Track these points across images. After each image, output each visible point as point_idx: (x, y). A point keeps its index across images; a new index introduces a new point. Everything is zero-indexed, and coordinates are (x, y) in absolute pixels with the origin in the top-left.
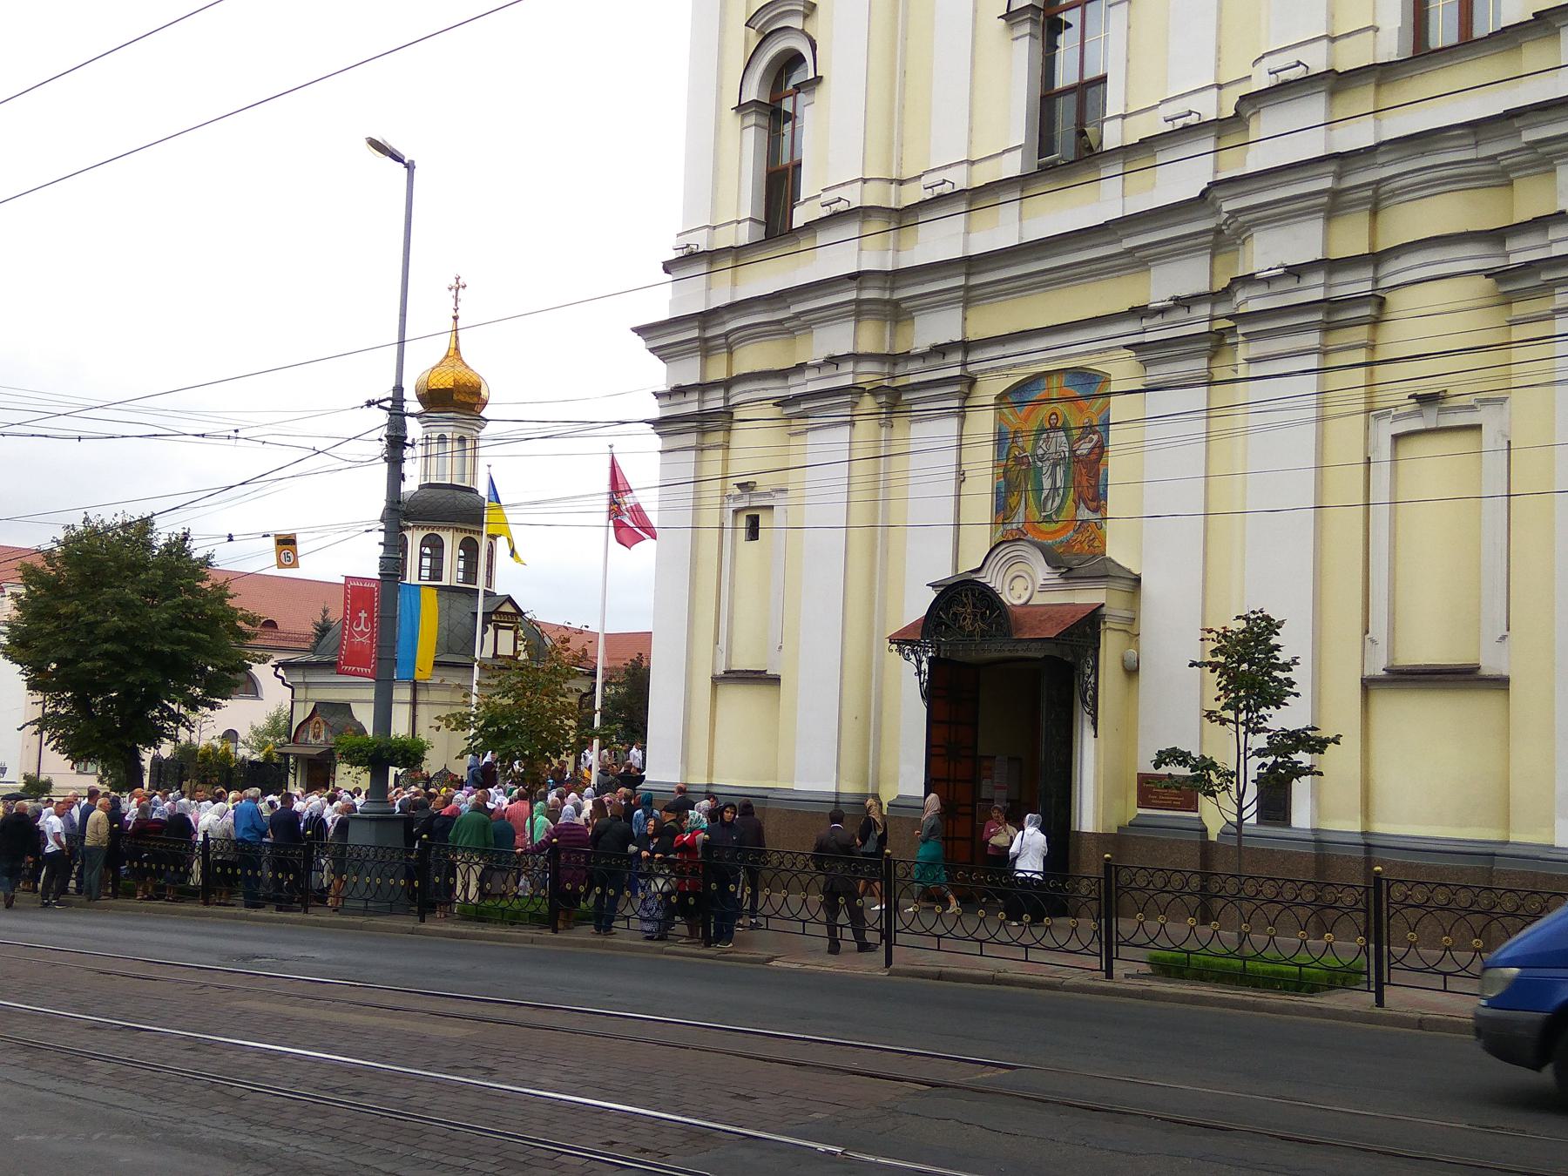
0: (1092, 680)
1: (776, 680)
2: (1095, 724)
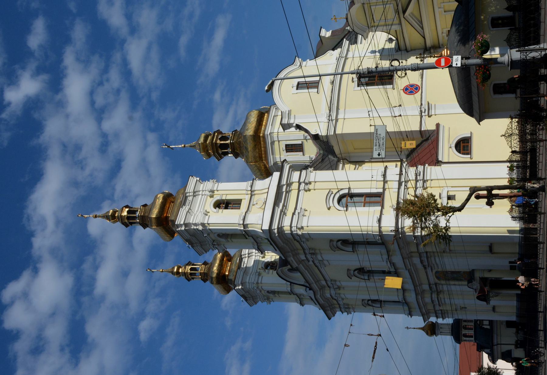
2: (502, 278)
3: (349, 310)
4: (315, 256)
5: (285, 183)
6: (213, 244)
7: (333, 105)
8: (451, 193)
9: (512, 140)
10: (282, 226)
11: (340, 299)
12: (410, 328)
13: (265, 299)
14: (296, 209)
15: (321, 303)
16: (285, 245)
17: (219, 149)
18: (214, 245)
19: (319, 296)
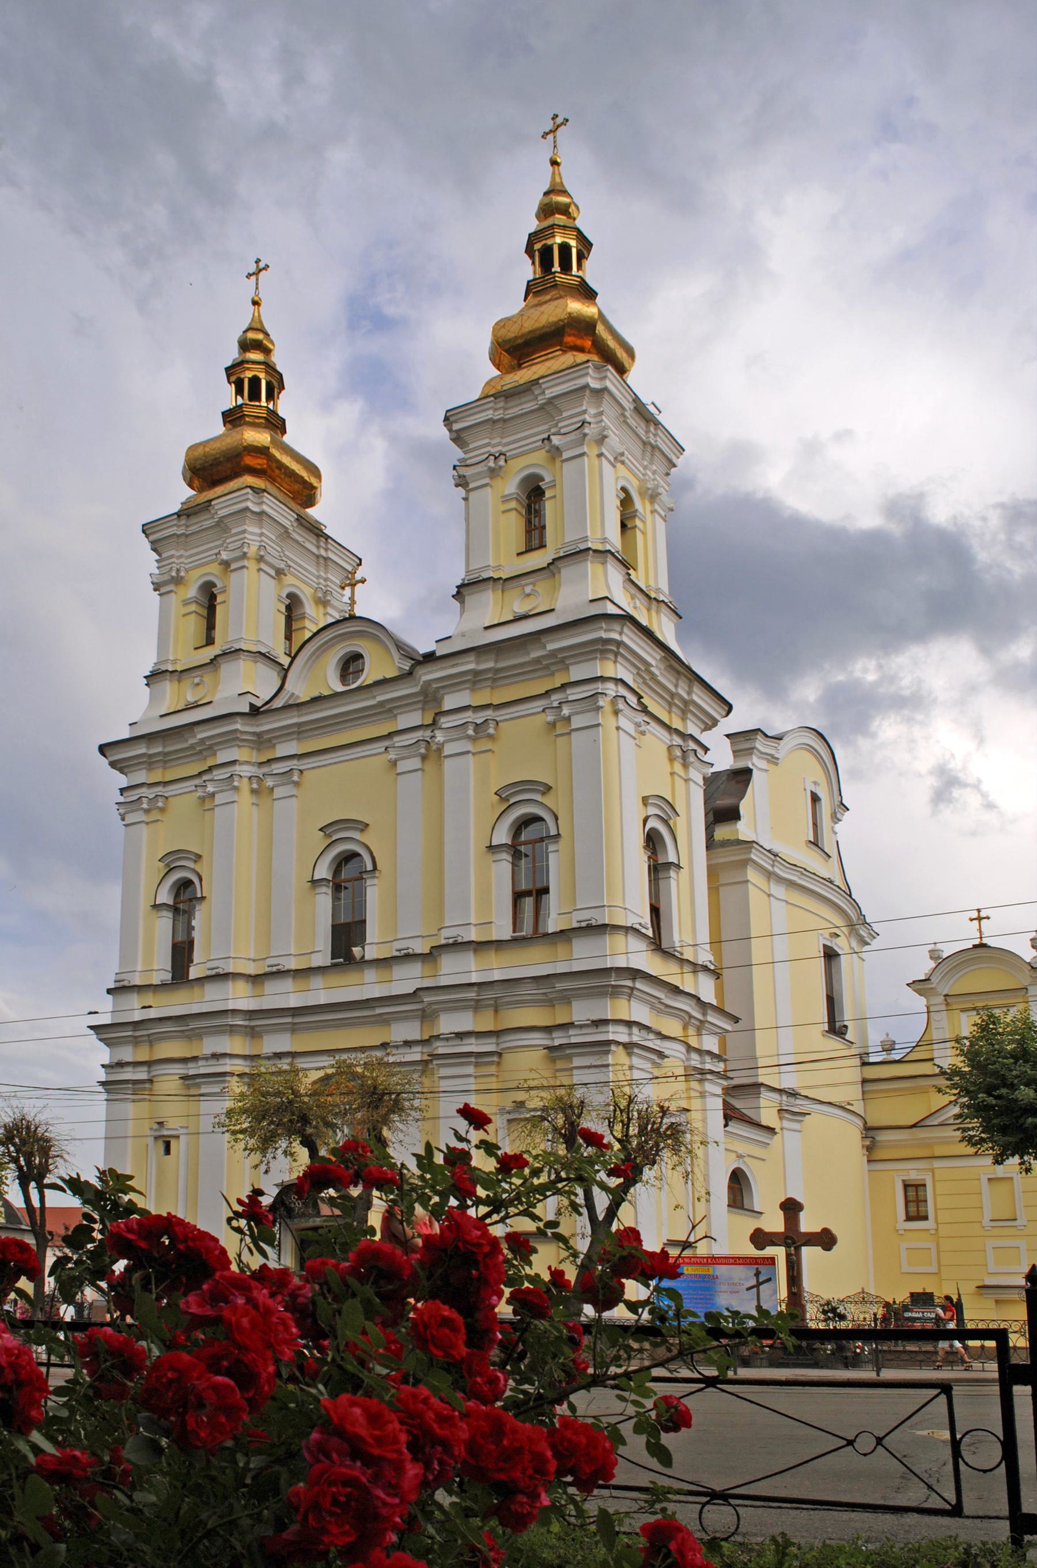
3: (142, 809)
4: (471, 732)
10: (619, 659)
11: (210, 789)
15: (197, 729)
16: (534, 655)
19: (238, 726)
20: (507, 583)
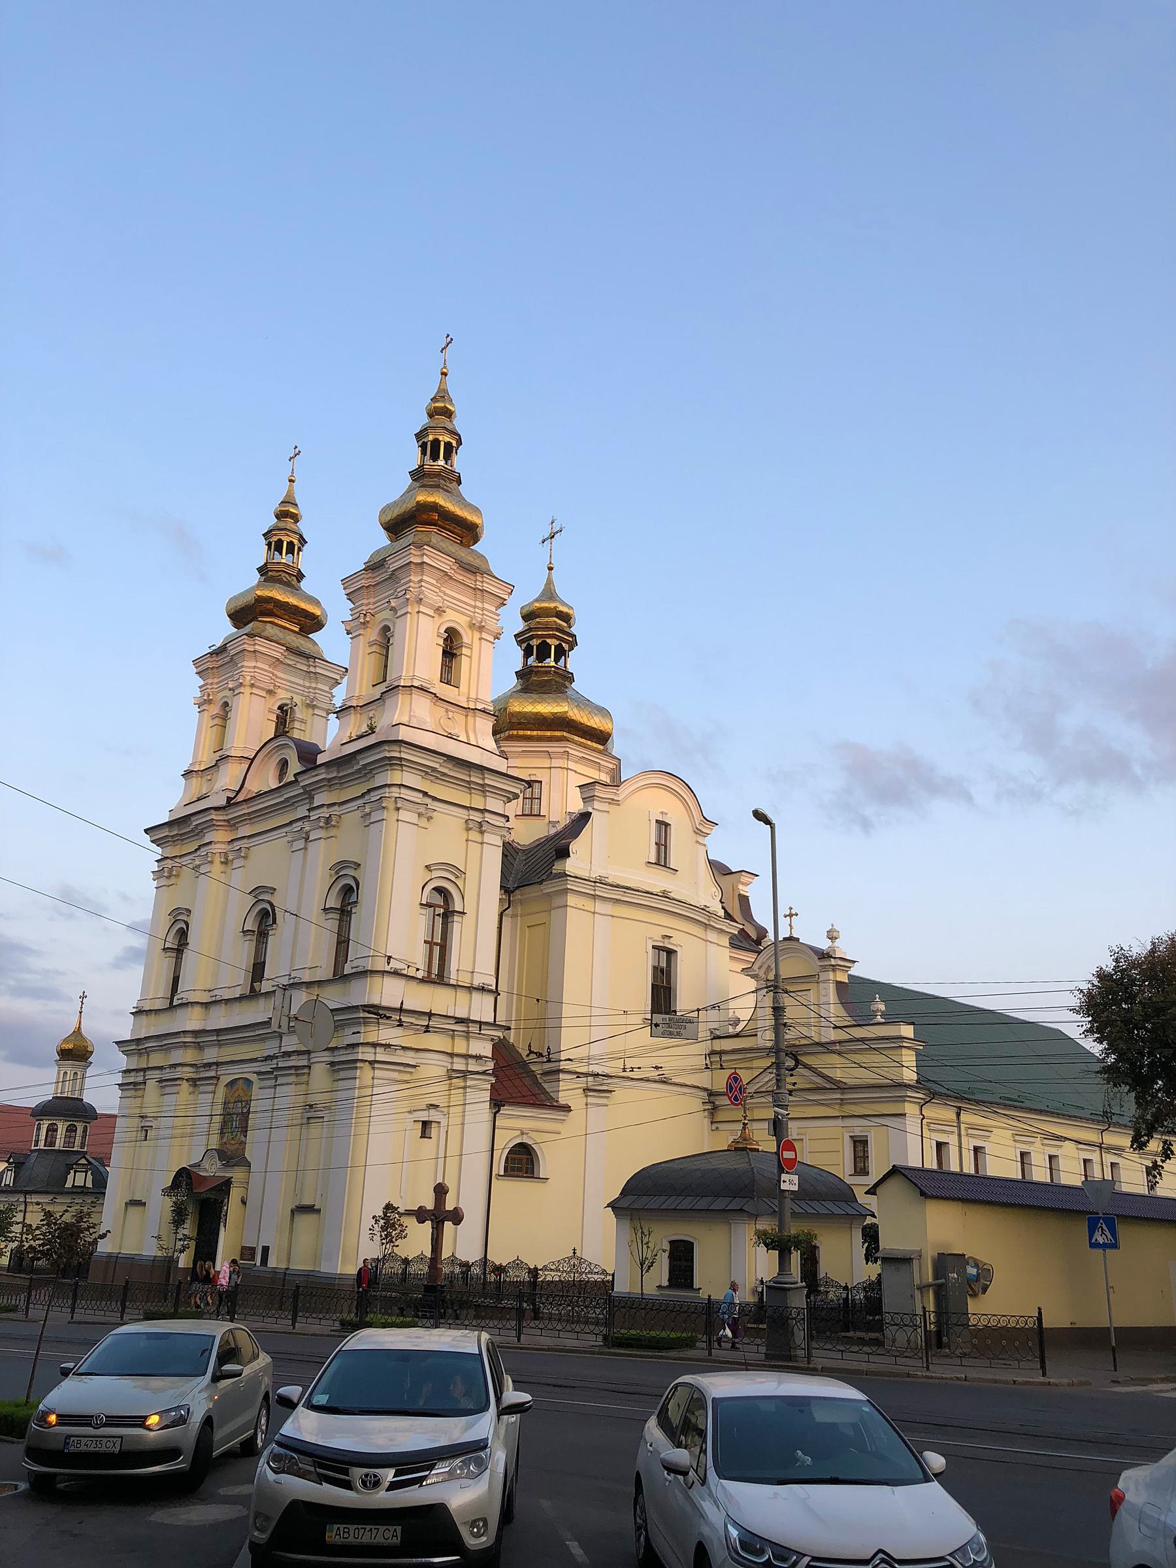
0: (225, 1208)
1: (144, 1204)
5: (487, 781)
6: (368, 614)
7: (623, 893)
8: (434, 1131)
9: (559, 1274)
10: (404, 768)
11: (197, 863)
12: (82, 1002)
13: (209, 695)
14: (434, 799)
17: (539, 642)
18: (365, 615)
20: (362, 708)
